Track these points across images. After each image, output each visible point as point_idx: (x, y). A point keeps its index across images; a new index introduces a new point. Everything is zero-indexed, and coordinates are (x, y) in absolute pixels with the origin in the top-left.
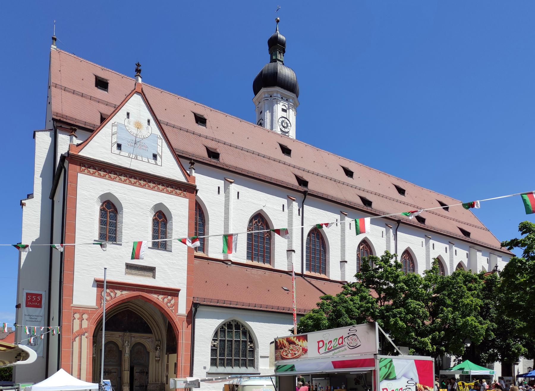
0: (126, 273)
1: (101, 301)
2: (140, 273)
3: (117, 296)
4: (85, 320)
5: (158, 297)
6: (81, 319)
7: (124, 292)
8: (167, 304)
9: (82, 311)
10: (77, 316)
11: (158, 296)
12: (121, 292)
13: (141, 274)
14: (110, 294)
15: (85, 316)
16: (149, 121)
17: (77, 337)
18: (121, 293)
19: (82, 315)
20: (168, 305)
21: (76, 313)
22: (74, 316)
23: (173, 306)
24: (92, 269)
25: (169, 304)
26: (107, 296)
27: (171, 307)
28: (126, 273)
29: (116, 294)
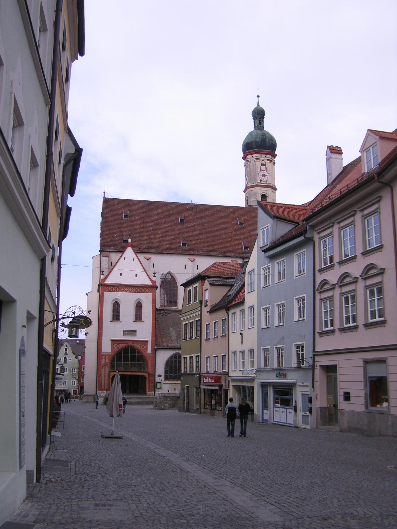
6: (105, 358)
7: (122, 344)
9: (106, 354)
14: (117, 346)
15: (107, 357)
16: (134, 258)
17: (103, 366)
28: (124, 335)
29: (119, 345)
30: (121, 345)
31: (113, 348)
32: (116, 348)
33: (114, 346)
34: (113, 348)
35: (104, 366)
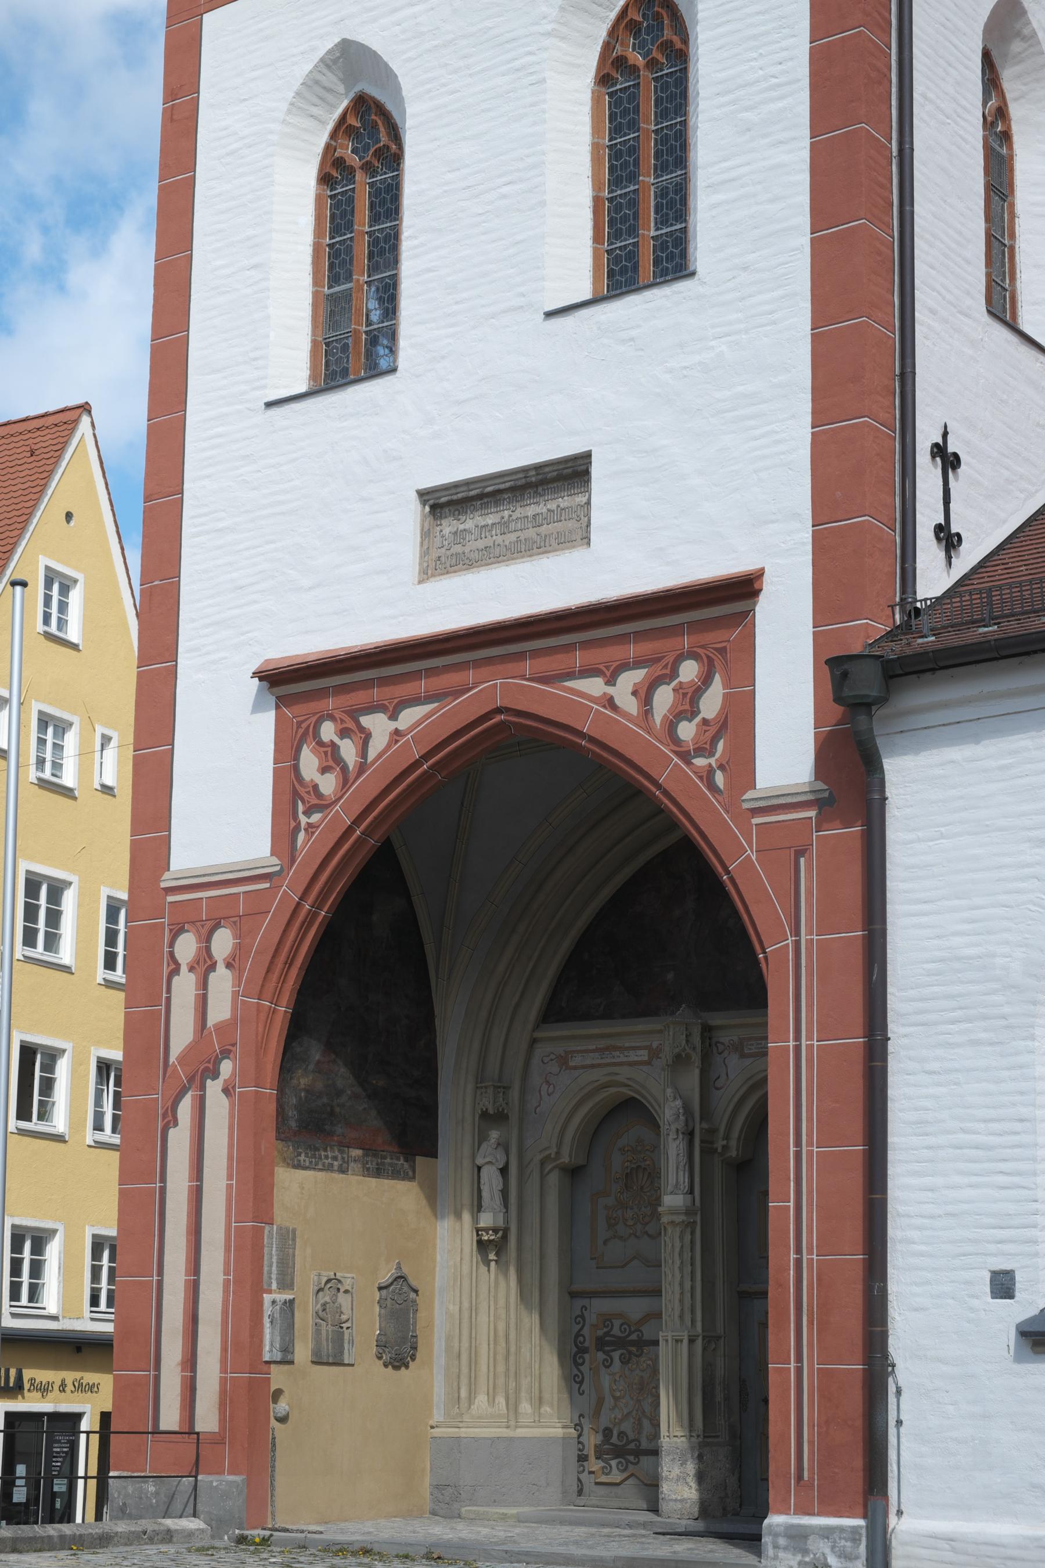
2: (512, 537)
3: (372, 754)
4: (221, 969)
5: (610, 690)
6: (204, 965)
7: (410, 716)
8: (671, 727)
10: (186, 947)
11: (611, 681)
13: (518, 540)
15: (223, 942)
18: (393, 725)
19: (208, 939)
20: (676, 741)
21: (181, 930)
22: (172, 954)
24: (255, 602)
25: (687, 731)
26: (324, 770)
27: (700, 751)
29: (365, 737)
30: (378, 725)
31: (296, 795)
32: (328, 784)
33: (309, 762)
35: (191, 1079)
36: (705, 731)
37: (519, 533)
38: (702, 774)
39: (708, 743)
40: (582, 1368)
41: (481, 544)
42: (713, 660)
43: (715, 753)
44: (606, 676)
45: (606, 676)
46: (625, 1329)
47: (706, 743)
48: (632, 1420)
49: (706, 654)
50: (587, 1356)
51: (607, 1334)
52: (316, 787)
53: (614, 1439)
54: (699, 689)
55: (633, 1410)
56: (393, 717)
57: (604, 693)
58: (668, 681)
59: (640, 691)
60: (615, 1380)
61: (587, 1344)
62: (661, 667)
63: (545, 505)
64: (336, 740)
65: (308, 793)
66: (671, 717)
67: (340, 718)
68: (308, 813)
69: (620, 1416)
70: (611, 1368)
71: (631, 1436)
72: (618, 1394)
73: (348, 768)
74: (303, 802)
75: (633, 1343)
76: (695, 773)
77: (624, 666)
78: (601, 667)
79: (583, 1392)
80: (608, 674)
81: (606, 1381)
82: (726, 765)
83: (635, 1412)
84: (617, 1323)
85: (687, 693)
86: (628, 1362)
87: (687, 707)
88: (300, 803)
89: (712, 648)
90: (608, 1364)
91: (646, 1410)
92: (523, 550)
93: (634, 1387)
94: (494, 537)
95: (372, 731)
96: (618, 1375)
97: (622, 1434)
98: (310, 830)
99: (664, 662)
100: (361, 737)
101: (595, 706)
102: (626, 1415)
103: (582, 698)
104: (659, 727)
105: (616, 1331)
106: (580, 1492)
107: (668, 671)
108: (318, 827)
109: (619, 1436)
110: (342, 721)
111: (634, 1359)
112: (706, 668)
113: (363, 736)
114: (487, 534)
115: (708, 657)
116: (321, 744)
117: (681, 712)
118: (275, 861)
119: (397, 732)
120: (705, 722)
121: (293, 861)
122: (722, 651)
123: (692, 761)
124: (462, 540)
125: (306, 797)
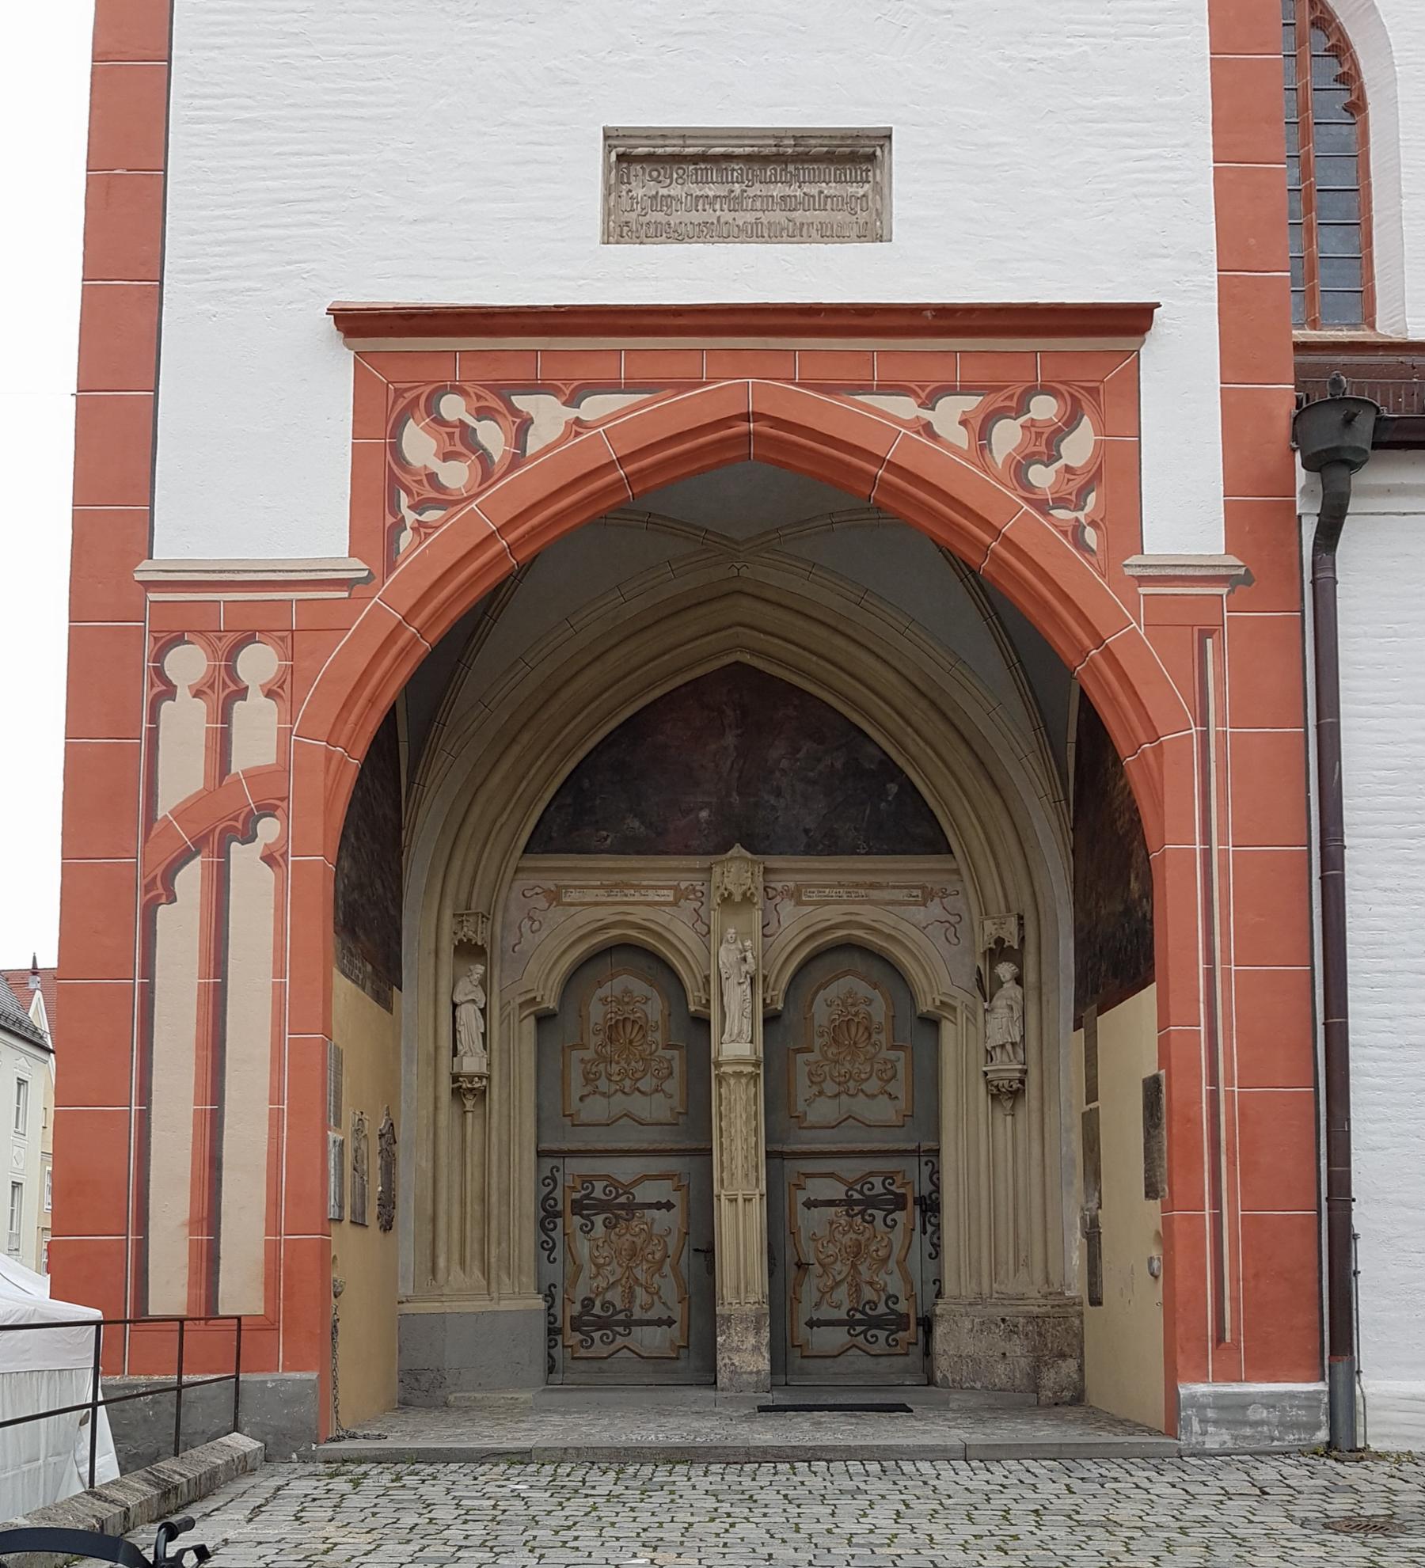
0: (617, 231)
1: (395, 508)
2: (750, 217)
3: (533, 445)
5: (926, 415)
11: (929, 403)
12: (573, 401)
20: (1028, 486)
23: (1083, 492)
25: (1042, 477)
26: (447, 457)
27: (1061, 502)
28: (617, 231)
29: (524, 425)
31: (394, 485)
32: (456, 475)
34: (394, 485)
36: (1069, 480)
37: (759, 214)
38: (1065, 529)
39: (1074, 493)
40: (553, 1234)
41: (696, 217)
42: (1080, 400)
43: (1085, 505)
44: (920, 397)
45: (920, 397)
46: (610, 1191)
47: (1070, 494)
48: (620, 1289)
49: (1069, 392)
50: (559, 1221)
51: (587, 1197)
52: (432, 477)
53: (597, 1310)
54: (1060, 429)
55: (621, 1279)
56: (573, 401)
57: (918, 417)
58: (1013, 415)
59: (972, 421)
60: (598, 1246)
61: (560, 1207)
62: (1002, 398)
63: (799, 187)
64: (471, 421)
65: (419, 482)
66: (1018, 458)
67: (476, 393)
68: (418, 507)
69: (604, 1285)
70: (591, 1233)
71: (619, 1306)
72: (601, 1261)
73: (491, 457)
74: (409, 492)
75: (622, 1206)
76: (1056, 526)
77: (949, 390)
78: (912, 385)
79: (555, 1259)
80: (923, 395)
81: (583, 1248)
82: (1101, 523)
83: (623, 1281)
84: (599, 1186)
85: (1043, 433)
86: (615, 1227)
87: (1043, 449)
88: (403, 494)
89: (1079, 386)
90: (587, 1230)
91: (640, 1278)
92: (766, 235)
93: (623, 1253)
94: (718, 213)
95: (534, 417)
96: (601, 1240)
97: (606, 1305)
98: (422, 530)
99: (1007, 392)
100: (514, 423)
101: (903, 431)
102: (612, 1284)
103: (882, 418)
104: (1000, 466)
105: (598, 1193)
106: (551, 1369)
107: (1013, 404)
108: (437, 528)
109: (602, 1306)
110: (479, 397)
111: (623, 1223)
112: (1069, 408)
113: (518, 421)
114: (707, 207)
115: (1072, 395)
116: (440, 421)
117: (1034, 454)
118: (357, 563)
119: (578, 421)
120: (1068, 469)
121: (391, 567)
122: (1093, 392)
123: (1051, 512)
124: (665, 208)
125: (415, 487)
